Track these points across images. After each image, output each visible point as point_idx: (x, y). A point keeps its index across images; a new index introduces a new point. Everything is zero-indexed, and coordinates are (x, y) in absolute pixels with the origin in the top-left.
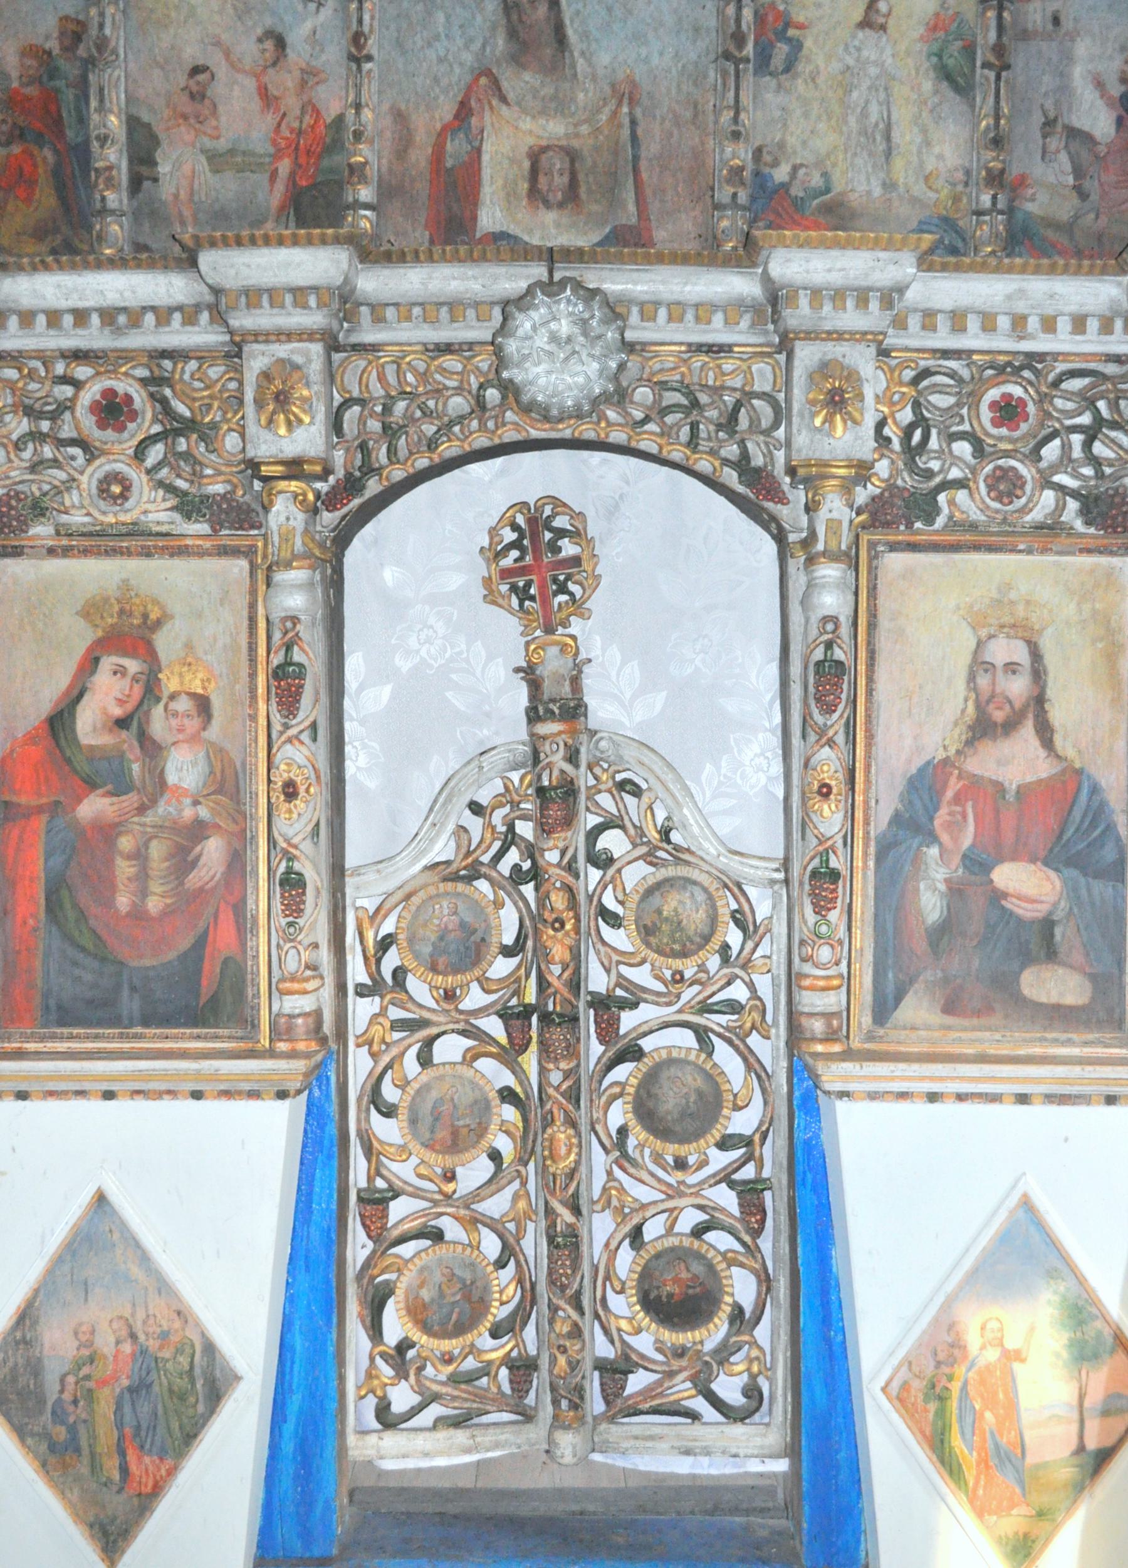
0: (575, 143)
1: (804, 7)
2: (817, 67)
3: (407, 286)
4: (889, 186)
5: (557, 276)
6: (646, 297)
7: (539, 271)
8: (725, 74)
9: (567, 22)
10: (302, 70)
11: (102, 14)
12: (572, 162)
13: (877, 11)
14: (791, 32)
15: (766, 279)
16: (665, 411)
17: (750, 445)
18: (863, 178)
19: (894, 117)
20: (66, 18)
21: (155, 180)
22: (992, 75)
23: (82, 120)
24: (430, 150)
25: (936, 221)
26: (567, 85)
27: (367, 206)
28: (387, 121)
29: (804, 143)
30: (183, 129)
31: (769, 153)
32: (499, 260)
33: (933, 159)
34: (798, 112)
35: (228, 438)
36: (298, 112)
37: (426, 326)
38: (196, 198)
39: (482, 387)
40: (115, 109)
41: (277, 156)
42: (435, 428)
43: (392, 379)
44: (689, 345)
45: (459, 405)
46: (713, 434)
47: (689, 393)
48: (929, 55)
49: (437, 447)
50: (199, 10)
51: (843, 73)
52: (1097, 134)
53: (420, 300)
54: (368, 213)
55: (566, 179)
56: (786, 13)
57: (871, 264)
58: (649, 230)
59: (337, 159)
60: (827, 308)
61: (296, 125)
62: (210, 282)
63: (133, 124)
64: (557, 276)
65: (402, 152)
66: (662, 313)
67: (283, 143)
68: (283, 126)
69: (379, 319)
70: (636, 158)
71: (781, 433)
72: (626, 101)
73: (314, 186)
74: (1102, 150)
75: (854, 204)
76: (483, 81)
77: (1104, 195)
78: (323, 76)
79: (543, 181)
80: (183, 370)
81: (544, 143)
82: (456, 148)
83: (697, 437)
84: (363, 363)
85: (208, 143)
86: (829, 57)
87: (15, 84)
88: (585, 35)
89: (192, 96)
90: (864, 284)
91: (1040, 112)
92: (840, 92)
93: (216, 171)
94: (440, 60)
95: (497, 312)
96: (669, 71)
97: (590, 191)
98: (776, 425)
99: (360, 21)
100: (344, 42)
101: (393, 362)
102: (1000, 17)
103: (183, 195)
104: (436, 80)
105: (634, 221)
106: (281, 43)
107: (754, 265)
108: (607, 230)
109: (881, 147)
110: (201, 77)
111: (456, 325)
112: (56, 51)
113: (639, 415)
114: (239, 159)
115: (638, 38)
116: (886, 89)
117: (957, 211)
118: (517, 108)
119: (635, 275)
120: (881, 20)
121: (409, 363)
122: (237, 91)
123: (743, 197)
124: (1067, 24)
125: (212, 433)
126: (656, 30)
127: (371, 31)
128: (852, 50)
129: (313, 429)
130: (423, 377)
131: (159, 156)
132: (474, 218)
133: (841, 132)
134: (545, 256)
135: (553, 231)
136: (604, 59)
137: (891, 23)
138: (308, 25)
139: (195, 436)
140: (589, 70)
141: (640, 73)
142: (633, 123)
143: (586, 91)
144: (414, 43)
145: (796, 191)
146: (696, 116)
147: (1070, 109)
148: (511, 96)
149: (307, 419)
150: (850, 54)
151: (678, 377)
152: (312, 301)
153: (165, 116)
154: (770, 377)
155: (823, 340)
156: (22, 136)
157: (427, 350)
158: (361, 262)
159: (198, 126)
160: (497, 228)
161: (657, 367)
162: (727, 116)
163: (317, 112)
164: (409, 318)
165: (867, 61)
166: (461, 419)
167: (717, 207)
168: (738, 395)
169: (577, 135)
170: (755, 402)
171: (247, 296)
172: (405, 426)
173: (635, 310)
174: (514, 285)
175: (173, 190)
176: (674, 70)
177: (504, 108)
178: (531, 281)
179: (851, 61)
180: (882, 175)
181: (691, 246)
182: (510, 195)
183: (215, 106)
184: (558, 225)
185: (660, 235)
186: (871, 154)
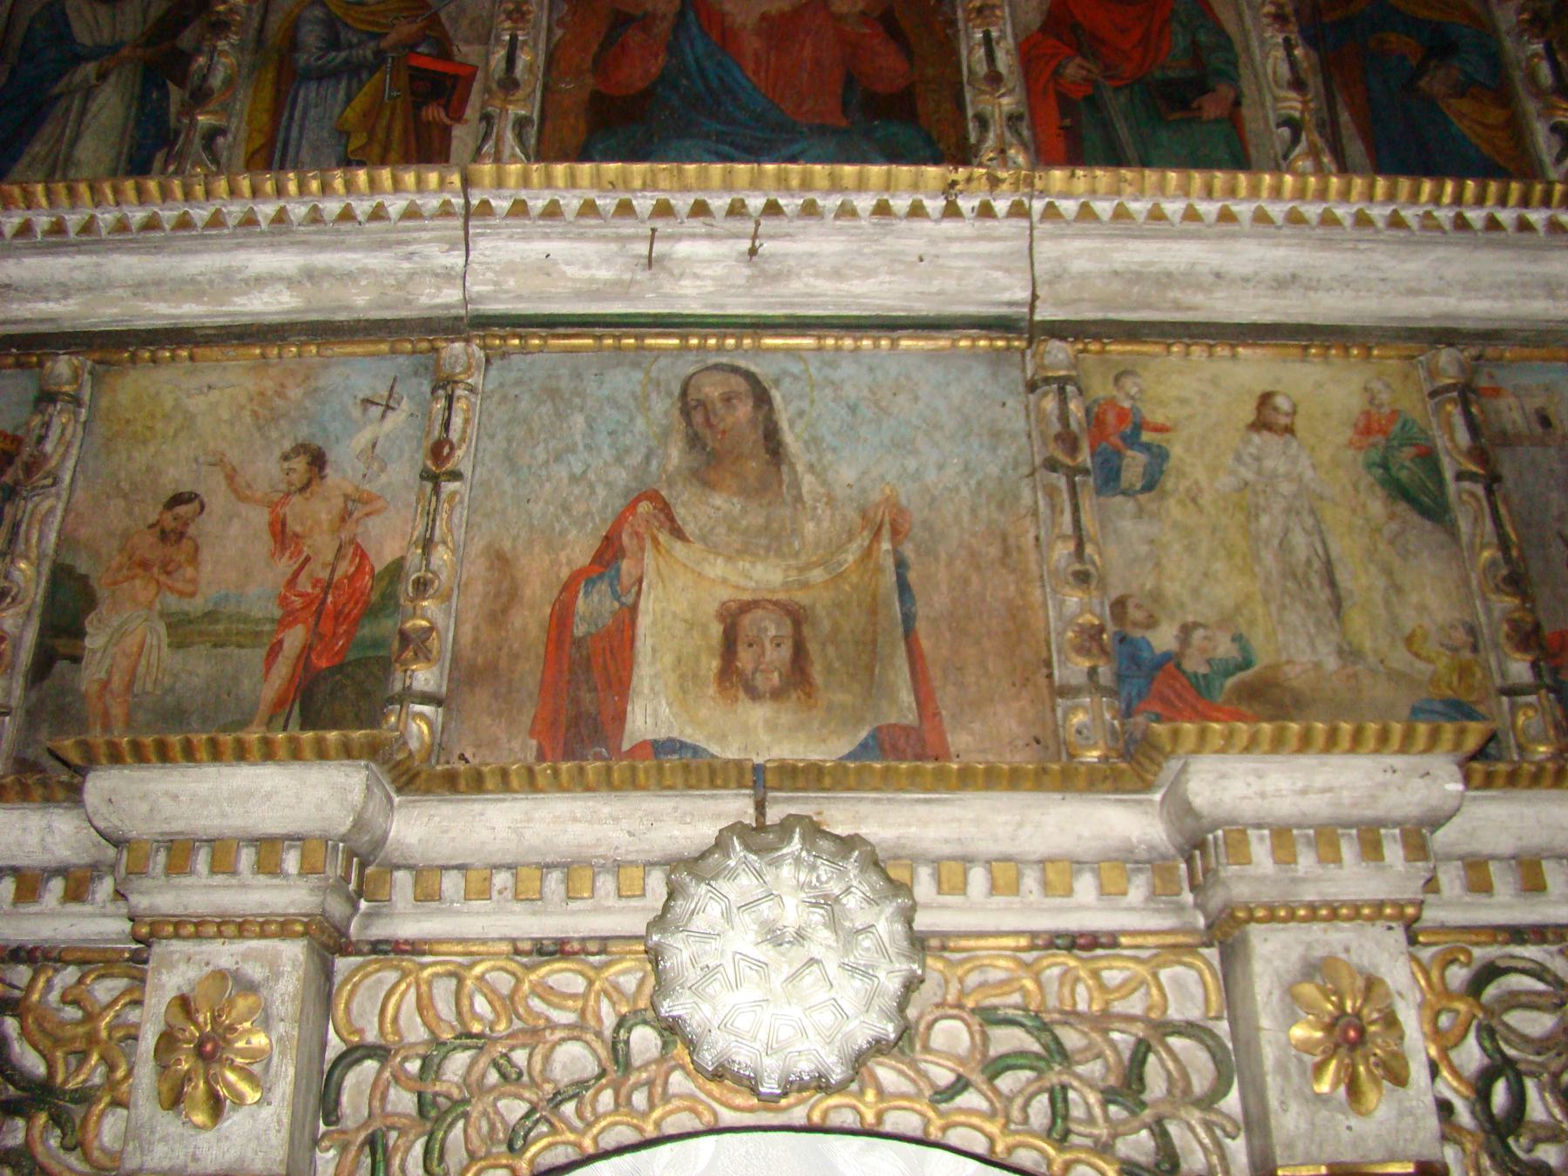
0: (801, 597)
1: (1161, 403)
2: (1197, 483)
3: (485, 834)
4: (1349, 653)
5: (774, 815)
6: (947, 850)
7: (737, 806)
8: (1051, 492)
9: (784, 425)
10: (347, 497)
11: (47, 425)
13: (1276, 409)
14: (1146, 437)
15: (1180, 810)
16: (996, 1067)
17: (1173, 1129)
18: (1303, 642)
19: (1334, 555)
21: (76, 659)
24: (548, 610)
25: (1439, 707)
26: (786, 512)
27: (426, 698)
28: (477, 568)
29: (1195, 592)
30: (138, 582)
31: (1138, 606)
32: (662, 785)
34: (1177, 547)
35: (109, 1121)
36: (330, 557)
37: (517, 907)
38: (137, 688)
39: (622, 1022)
40: (33, 555)
42: (523, 1107)
43: (445, 1008)
44: (1034, 935)
45: (574, 1059)
46: (1097, 1111)
47: (1041, 1027)
48: (1369, 466)
49: (525, 1147)
50: (199, 419)
51: (1240, 490)
53: (509, 859)
54: (427, 709)
55: (786, 652)
56: (1135, 410)
57: (1380, 777)
58: (941, 735)
59: (386, 626)
60: (1306, 861)
61: (324, 575)
62: (102, 825)
64: (774, 815)
66: (978, 876)
67: (298, 602)
69: (427, 895)
70: (908, 619)
71: (1232, 1101)
72: (886, 532)
73: (340, 668)
75: (1295, 683)
76: (644, 507)
78: (379, 504)
79: (745, 658)
80: (49, 985)
81: (747, 597)
82: (592, 607)
83: (1066, 1117)
84: (391, 976)
85: (173, 602)
86: (1213, 470)
88: (814, 442)
89: (164, 536)
90: (1369, 814)
91: (1559, 541)
92: (1240, 517)
93: (179, 644)
94: (574, 479)
95: (657, 883)
96: (957, 489)
97: (829, 670)
98: (1220, 1089)
99: (446, 425)
100: (420, 456)
101: (451, 974)
103: (117, 683)
104: (566, 508)
105: (911, 718)
106: (318, 460)
107: (1148, 787)
108: (863, 734)
109: (1324, 595)
110: (182, 510)
111: (574, 905)
113: (944, 1077)
114: (220, 627)
115: (901, 445)
116: (1312, 512)
117: (1470, 688)
118: (698, 546)
119: (922, 810)
120: (1283, 421)
121: (481, 978)
122: (235, 528)
123: (1105, 673)
125: (78, 1111)
126: (927, 433)
127: (463, 439)
128: (1248, 459)
129: (266, 1112)
130: (508, 1003)
131: (90, 624)
132: (620, 717)
133: (1254, 575)
134: (749, 778)
135: (765, 738)
136: (846, 474)
137: (1300, 423)
138: (363, 438)
139: (42, 1118)
140: (822, 490)
141: (907, 494)
142: (901, 565)
143: (818, 522)
144: (533, 457)
146: (1006, 552)
148: (690, 528)
149: (252, 1096)
150: (1245, 465)
151: (1016, 998)
152: (291, 862)
153: (114, 564)
154: (1197, 991)
155: (1304, 920)
157: (517, 952)
158: (399, 791)
159: (163, 578)
160: (662, 734)
161: (973, 979)
162: (1062, 551)
163: (362, 555)
164: (485, 894)
165: (1274, 475)
166: (579, 1089)
167: (1065, 691)
168: (1139, 1030)
169: (805, 585)
170: (1173, 1041)
171: (169, 850)
172: (465, 1101)
173: (924, 873)
174: (689, 831)
175: (103, 675)
176: (964, 491)
177: (678, 546)
178: (724, 824)
179: (1250, 476)
181: (1024, 759)
182: (687, 679)
183: (197, 549)
184: (772, 727)
185: (959, 740)
186: (1310, 606)
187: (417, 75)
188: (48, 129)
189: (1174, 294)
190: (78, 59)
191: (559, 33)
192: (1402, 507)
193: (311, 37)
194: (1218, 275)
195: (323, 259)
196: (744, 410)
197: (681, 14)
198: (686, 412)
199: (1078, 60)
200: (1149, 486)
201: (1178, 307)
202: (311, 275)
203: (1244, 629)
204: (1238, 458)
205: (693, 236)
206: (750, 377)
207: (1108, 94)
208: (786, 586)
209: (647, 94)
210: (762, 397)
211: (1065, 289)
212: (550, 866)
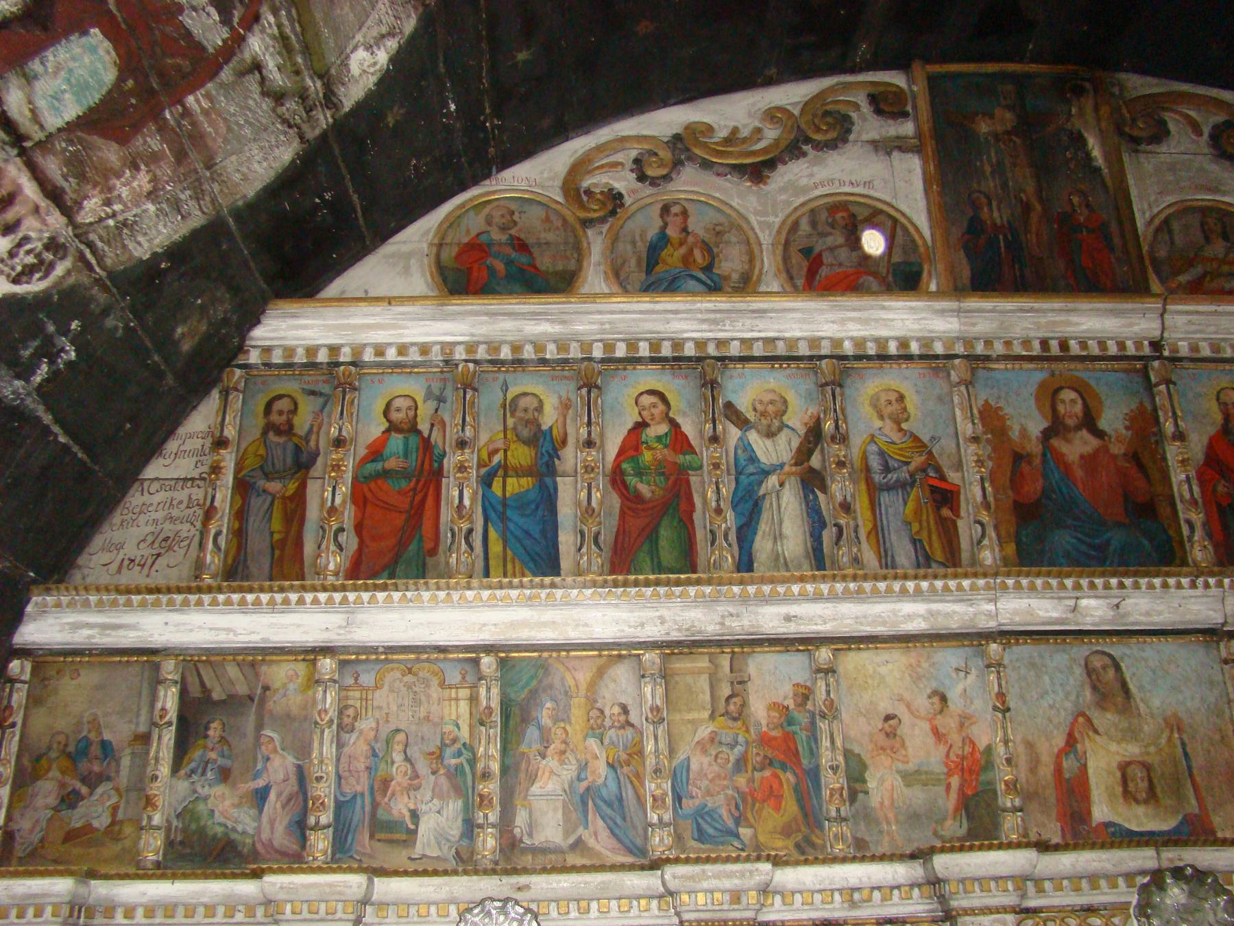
0: (1148, 759)
3: (1061, 867)
9: (1128, 680)
20: (798, 685)
21: (867, 793)
23: (814, 753)
24: (1052, 767)
28: (1021, 749)
41: (949, 774)
58: (1208, 816)
63: (847, 754)
65: (1033, 770)
67: (953, 765)
68: (951, 755)
70: (1190, 768)
73: (976, 795)
76: (1081, 719)
79: (1131, 787)
82: (1069, 764)
85: (901, 766)
87: (765, 729)
88: (1141, 688)
89: (887, 735)
93: (908, 785)
94: (1051, 707)
96: (1199, 709)
103: (886, 803)
104: (1051, 721)
105: (1197, 811)
106: (944, 699)
108: (1180, 818)
110: (891, 722)
112: (792, 706)
114: (923, 777)
122: (917, 731)
131: (867, 775)
132: (1089, 813)
135: (1145, 820)
136: (1156, 703)
138: (960, 687)
142: (1183, 744)
146: (1223, 738)
148: (1101, 730)
152: (1010, 886)
156: (771, 764)
160: (1107, 820)
163: (972, 743)
169: (1148, 754)
177: (1097, 737)
182: (1111, 796)
183: (903, 741)
184: (1146, 815)
188: (765, 516)
190: (766, 473)
193: (875, 463)
195: (935, 606)
196: (1111, 673)
197: (1044, 455)
198: (1089, 674)
199: (1223, 482)
202: (931, 613)
205: (1089, 597)
206: (1110, 656)
208: (1141, 754)
210: (1117, 667)
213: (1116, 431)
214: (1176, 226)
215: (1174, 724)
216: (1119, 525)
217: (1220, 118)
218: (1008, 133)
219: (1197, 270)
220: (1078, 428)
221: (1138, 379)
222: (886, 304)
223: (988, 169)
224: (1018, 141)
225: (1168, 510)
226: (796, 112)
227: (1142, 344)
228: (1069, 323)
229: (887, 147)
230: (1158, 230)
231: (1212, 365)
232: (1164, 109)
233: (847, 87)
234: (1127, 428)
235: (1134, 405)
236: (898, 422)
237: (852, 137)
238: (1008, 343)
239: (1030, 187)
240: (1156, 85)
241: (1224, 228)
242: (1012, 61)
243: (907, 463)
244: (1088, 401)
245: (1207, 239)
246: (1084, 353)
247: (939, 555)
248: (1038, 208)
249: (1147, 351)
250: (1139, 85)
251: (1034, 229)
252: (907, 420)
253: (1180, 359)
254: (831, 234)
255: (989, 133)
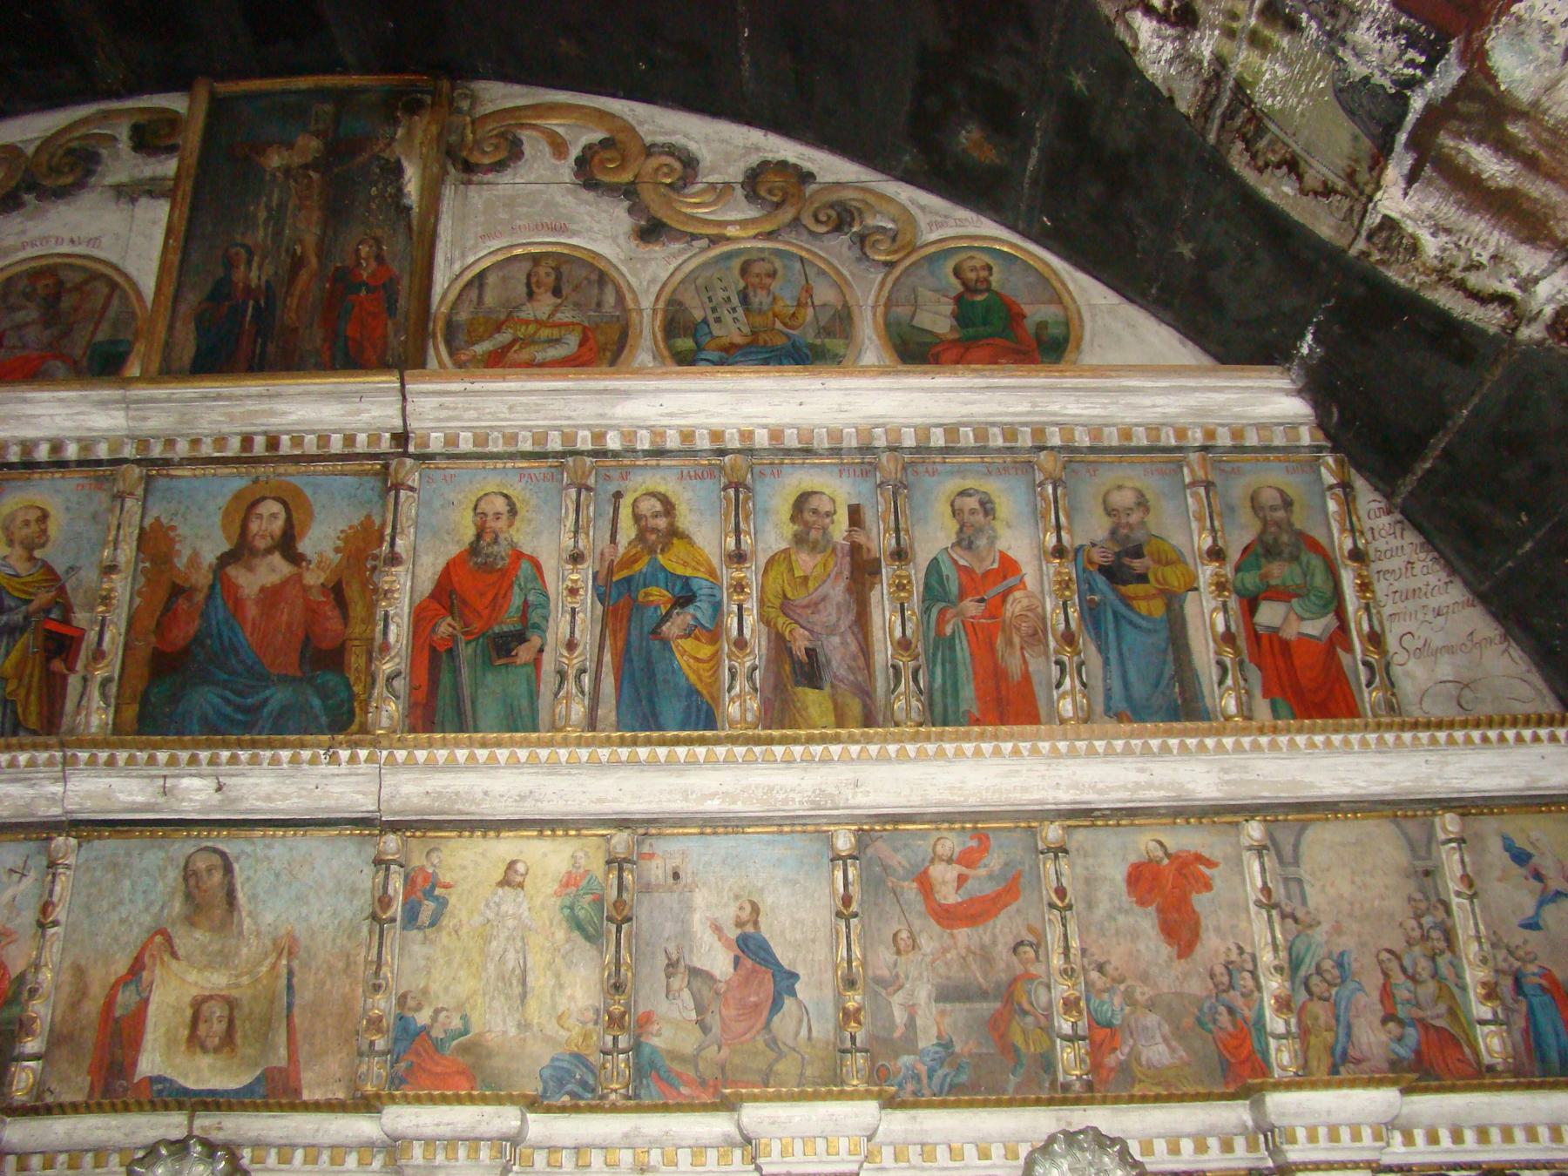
0: (235, 993)
1: (451, 870)
4: (524, 1026)
9: (238, 887)
12: (231, 1009)
14: (438, 891)
18: (499, 1020)
22: (613, 928)
25: (567, 1057)
26: (233, 942)
28: (66, 977)
29: (446, 989)
33: (565, 1000)
34: (442, 961)
52: (717, 973)
55: (224, 1025)
56: (434, 874)
58: (298, 1073)
59: (16, 1010)
65: (75, 1005)
70: (290, 1006)
72: (285, 952)
74: (722, 987)
77: (725, 1027)
79: (202, 1029)
82: (126, 999)
88: (253, 898)
94: (122, 921)
96: (325, 927)
97: (245, 1036)
102: (620, 878)
104: (116, 939)
109: (517, 990)
116: (523, 939)
118: (184, 963)
120: (519, 879)
124: (686, 877)
132: (134, 1064)
136: (269, 918)
137: (528, 880)
141: (300, 930)
142: (291, 974)
145: (437, 1033)
146: (348, 965)
147: (691, 951)
148: (181, 952)
160: (156, 1073)
169: (238, 986)
179: (490, 915)
180: (517, 1016)
182: (171, 1042)
184: (212, 1067)
186: (508, 997)
187: (50, 635)
189: (459, 806)
191: (138, 600)
192: (576, 934)
194: (486, 793)
196: (218, 876)
197: (212, 587)
198: (186, 879)
199: (449, 619)
200: (432, 924)
201: (460, 812)
203: (468, 1011)
204: (487, 905)
205: (191, 775)
206: (223, 855)
207: (462, 646)
208: (228, 986)
209: (186, 651)
210: (228, 869)
211: (396, 804)
212: (87, 1151)
213: (321, 554)
214: (492, 279)
215: (287, 947)
216: (285, 679)
217: (597, 136)
218: (306, 167)
219: (505, 337)
220: (269, 551)
221: (372, 483)
222: (29, 395)
223: (262, 215)
224: (314, 175)
225: (362, 662)
226: (30, 150)
227: (379, 438)
228: (272, 413)
229: (128, 193)
230: (469, 284)
231: (479, 464)
232: (522, 126)
233: (106, 116)
234: (337, 550)
235: (357, 518)
236: (29, 547)
237: (93, 180)
238: (196, 442)
239: (311, 236)
240: (522, 96)
241: (559, 278)
242: (332, 72)
243: (27, 602)
244: (295, 515)
245: (531, 295)
246: (297, 452)
247: (33, 721)
248: (314, 261)
249: (385, 445)
250: (497, 95)
251: (297, 293)
252: (43, 546)
253: (432, 457)
254: (25, 307)
255: (278, 169)
